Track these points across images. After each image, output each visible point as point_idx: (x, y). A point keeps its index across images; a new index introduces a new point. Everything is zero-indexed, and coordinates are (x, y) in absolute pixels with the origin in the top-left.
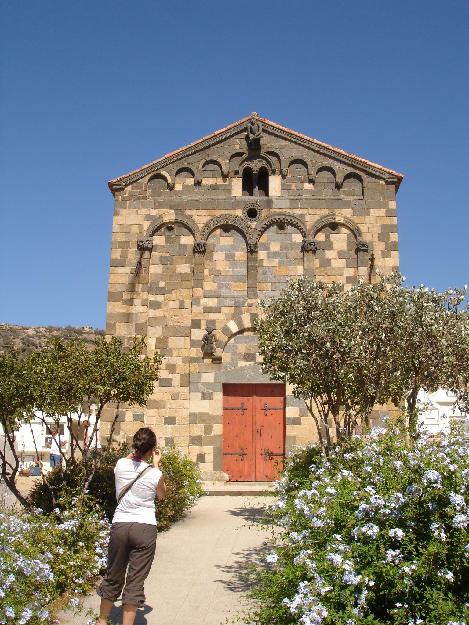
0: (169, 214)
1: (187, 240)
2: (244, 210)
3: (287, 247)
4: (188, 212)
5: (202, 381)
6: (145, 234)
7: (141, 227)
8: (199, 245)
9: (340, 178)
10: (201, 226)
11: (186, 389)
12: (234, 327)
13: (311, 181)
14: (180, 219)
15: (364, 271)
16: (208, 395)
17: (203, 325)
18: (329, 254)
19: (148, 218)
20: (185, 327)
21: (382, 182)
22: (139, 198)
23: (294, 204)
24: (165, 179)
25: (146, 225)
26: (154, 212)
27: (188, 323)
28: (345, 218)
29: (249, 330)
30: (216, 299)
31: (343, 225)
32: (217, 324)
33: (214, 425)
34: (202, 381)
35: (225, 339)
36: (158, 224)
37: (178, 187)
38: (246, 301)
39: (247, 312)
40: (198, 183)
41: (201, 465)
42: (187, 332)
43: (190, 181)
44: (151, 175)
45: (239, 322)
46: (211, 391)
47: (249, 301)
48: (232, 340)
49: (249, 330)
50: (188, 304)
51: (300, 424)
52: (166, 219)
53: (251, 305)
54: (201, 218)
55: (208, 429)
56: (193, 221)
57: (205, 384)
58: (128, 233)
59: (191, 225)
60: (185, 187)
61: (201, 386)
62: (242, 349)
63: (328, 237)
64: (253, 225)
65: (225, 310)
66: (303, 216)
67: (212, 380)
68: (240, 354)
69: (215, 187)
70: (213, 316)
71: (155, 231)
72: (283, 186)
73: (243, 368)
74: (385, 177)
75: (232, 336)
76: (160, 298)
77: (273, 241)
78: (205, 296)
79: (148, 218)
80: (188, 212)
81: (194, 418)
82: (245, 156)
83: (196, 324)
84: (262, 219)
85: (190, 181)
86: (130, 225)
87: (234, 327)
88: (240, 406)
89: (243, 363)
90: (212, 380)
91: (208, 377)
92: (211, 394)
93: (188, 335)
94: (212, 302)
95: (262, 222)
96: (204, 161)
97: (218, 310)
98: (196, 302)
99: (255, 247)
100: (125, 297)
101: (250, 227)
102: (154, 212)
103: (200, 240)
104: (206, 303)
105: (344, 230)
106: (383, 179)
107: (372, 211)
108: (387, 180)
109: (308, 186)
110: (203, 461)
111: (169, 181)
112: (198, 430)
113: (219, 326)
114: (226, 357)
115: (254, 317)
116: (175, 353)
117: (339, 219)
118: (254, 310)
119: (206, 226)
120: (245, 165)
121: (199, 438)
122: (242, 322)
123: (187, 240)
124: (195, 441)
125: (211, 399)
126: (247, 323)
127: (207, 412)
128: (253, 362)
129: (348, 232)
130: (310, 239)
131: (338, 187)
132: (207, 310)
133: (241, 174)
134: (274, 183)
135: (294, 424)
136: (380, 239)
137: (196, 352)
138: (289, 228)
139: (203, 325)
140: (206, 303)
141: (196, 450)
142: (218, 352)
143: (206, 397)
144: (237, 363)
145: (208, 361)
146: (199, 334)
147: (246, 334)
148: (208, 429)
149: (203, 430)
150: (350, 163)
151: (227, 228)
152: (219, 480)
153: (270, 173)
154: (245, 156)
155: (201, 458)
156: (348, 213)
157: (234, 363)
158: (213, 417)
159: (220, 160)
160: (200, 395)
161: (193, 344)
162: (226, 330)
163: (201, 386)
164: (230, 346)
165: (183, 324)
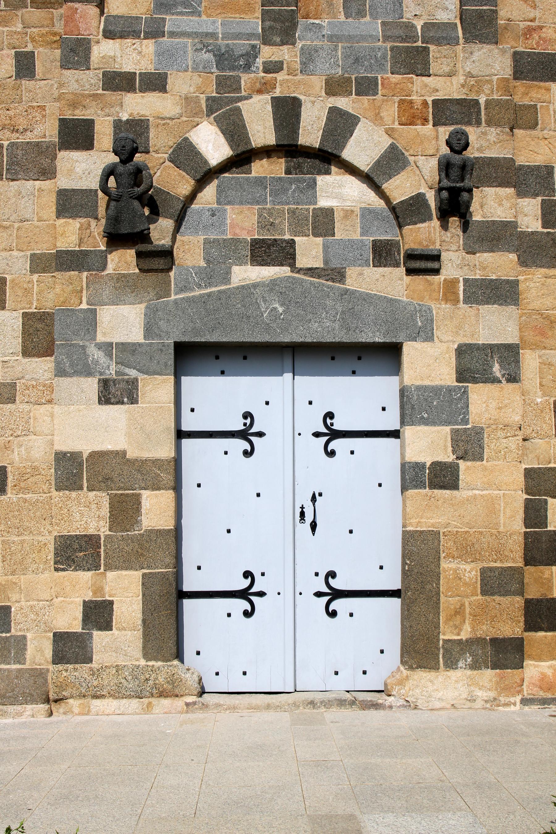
5: (100, 338)
11: (42, 368)
12: (213, 146)
16: (123, 385)
17: (104, 136)
20: (38, 144)
27: (47, 131)
29: (267, 152)
30: (149, 47)
32: (152, 134)
33: (145, 494)
34: (100, 338)
35: (182, 185)
38: (254, 52)
39: (260, 92)
41: (99, 638)
42: (45, 162)
45: (233, 128)
46: (133, 373)
47: (268, 53)
48: (210, 192)
49: (267, 152)
50: (47, 58)
51: (454, 485)
53: (273, 67)
55: (125, 511)
57: (107, 348)
62: (243, 222)
65: (182, 83)
67: (136, 335)
68: (236, 241)
70: (136, 105)
73: (247, 290)
75: (206, 176)
78: (109, 34)
81: (71, 470)
83: (77, 135)
88: (238, 426)
89: (246, 274)
90: (136, 335)
91: (123, 322)
93: (48, 173)
94: (133, 56)
97: (156, 83)
98: (76, 53)
104: (114, 58)
110: (107, 626)
112: (89, 513)
114: (190, 251)
115: (287, 111)
118: (284, 85)
121: (91, 542)
122: (244, 126)
124: (75, 552)
125: (133, 400)
126: (262, 130)
127: (118, 447)
128: (284, 271)
135: (433, 486)
139: (104, 136)
140: (114, 58)
141: (80, 585)
142: (161, 231)
143: (114, 393)
144: (228, 272)
145: (123, 261)
146: (84, 169)
147: (260, 168)
148: (125, 511)
149: (105, 511)
152: (163, 694)
155: (99, 614)
157: (216, 270)
158: (141, 465)
160: (91, 385)
161: (70, 203)
162: (185, 155)
163: (95, 354)
164: (199, 213)
165: (29, 137)
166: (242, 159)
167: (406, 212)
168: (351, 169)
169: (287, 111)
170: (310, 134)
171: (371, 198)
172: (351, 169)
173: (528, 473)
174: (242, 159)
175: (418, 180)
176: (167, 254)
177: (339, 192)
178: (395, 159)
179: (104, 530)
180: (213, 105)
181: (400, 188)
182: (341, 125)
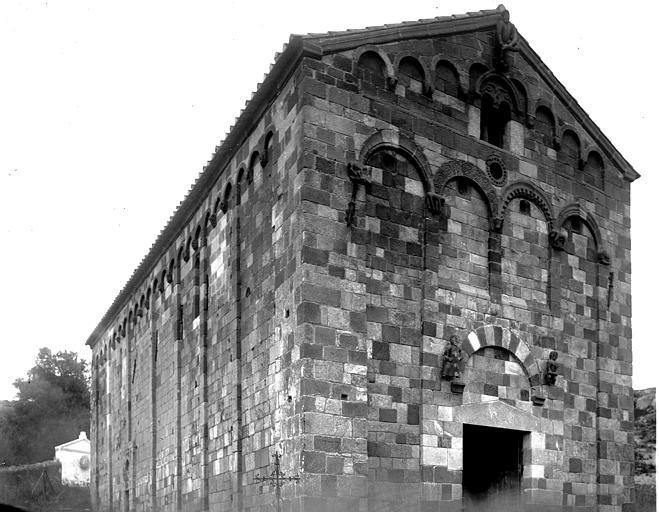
4: (421, 140)
6: (357, 155)
7: (351, 141)
10: (434, 170)
12: (476, 345)
13: (557, 147)
14: (408, 147)
15: (603, 292)
18: (573, 260)
19: (363, 129)
21: (621, 176)
25: (359, 140)
45: (482, 337)
54: (434, 155)
56: (424, 157)
61: (437, 426)
69: (448, 111)
70: (450, 319)
74: (626, 170)
76: (378, 276)
79: (363, 129)
80: (421, 140)
84: (508, 184)
87: (476, 345)
92: (450, 439)
95: (508, 188)
100: (332, 261)
103: (432, 193)
105: (585, 229)
106: (623, 172)
108: (627, 175)
115: (499, 332)
119: (441, 172)
131: (581, 166)
132: (445, 309)
137: (428, 373)
146: (436, 346)
150: (597, 137)
151: (464, 185)
169: (499, 332)
170: (506, 343)
174: (481, 351)
177: (511, 368)
178: (529, 359)
181: (533, 370)
182: (515, 342)
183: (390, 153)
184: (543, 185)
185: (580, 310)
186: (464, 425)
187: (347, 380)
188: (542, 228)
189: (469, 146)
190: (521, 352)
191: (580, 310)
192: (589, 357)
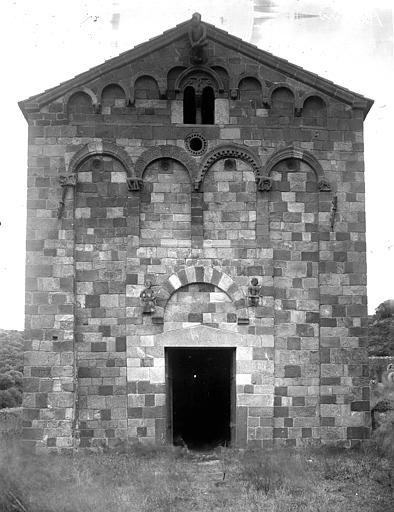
0: (96, 144)
1: (119, 177)
2: (186, 140)
3: (237, 188)
4: (119, 142)
7: (62, 160)
8: (132, 182)
9: (299, 103)
10: (134, 160)
12: (176, 283)
14: (110, 150)
18: (287, 197)
19: (71, 148)
21: (349, 108)
22: (58, 123)
23: (245, 134)
24: (89, 98)
26: (76, 142)
28: (304, 152)
31: (302, 160)
36: (83, 155)
37: (107, 111)
40: (131, 105)
43: (120, 103)
44: (71, 93)
45: (182, 278)
52: (92, 150)
56: (126, 153)
58: (47, 168)
59: (123, 158)
60: (115, 111)
61: (140, 351)
63: (284, 177)
64: (198, 159)
66: (255, 149)
69: (150, 112)
70: (151, 269)
71: (79, 166)
72: (232, 113)
77: (222, 176)
79: (71, 148)
80: (119, 142)
82: (186, 72)
84: (208, 151)
85: (120, 103)
86: (48, 159)
87: (176, 283)
92: (152, 360)
95: (207, 156)
96: (137, 76)
99: (199, 186)
100: (46, 246)
101: (193, 161)
102: (76, 142)
105: (304, 167)
106: (350, 104)
107: (335, 144)
108: (355, 106)
109: (261, 112)
111: (95, 101)
113: (159, 281)
115: (200, 271)
116: (108, 313)
117: (299, 155)
119: (141, 160)
120: (187, 84)
123: (119, 177)
124: (135, 413)
129: (309, 169)
130: (264, 177)
132: (146, 262)
133: (182, 95)
134: (221, 107)
136: (344, 180)
137: (131, 311)
138: (240, 165)
139: (141, 278)
142: (159, 311)
146: (135, 292)
153: (216, 94)
154: (186, 72)
156: (308, 146)
159: (156, 77)
162: (168, 285)
166: (184, 288)
167: (241, 304)
168: (221, 291)
169: (200, 271)
170: (208, 277)
171: (228, 299)
172: (221, 291)
173: (276, 389)
174: (184, 288)
175: (242, 293)
176: (162, 319)
177: (215, 297)
178: (233, 289)
179: (143, 406)
180: (176, 269)
181: (237, 297)
182: (217, 276)
183: (98, 158)
184: (247, 142)
185: (297, 237)
186: (166, 348)
187: (57, 326)
188: (250, 177)
189: (177, 134)
190: (225, 282)
191: (297, 237)
192: (309, 275)
